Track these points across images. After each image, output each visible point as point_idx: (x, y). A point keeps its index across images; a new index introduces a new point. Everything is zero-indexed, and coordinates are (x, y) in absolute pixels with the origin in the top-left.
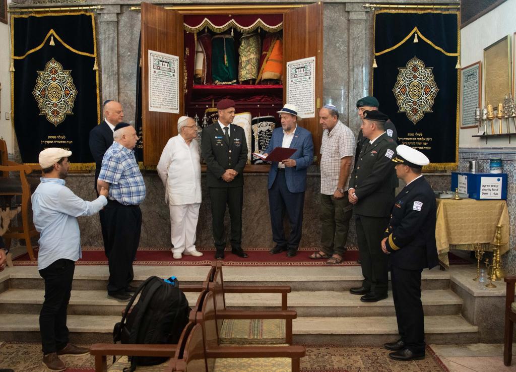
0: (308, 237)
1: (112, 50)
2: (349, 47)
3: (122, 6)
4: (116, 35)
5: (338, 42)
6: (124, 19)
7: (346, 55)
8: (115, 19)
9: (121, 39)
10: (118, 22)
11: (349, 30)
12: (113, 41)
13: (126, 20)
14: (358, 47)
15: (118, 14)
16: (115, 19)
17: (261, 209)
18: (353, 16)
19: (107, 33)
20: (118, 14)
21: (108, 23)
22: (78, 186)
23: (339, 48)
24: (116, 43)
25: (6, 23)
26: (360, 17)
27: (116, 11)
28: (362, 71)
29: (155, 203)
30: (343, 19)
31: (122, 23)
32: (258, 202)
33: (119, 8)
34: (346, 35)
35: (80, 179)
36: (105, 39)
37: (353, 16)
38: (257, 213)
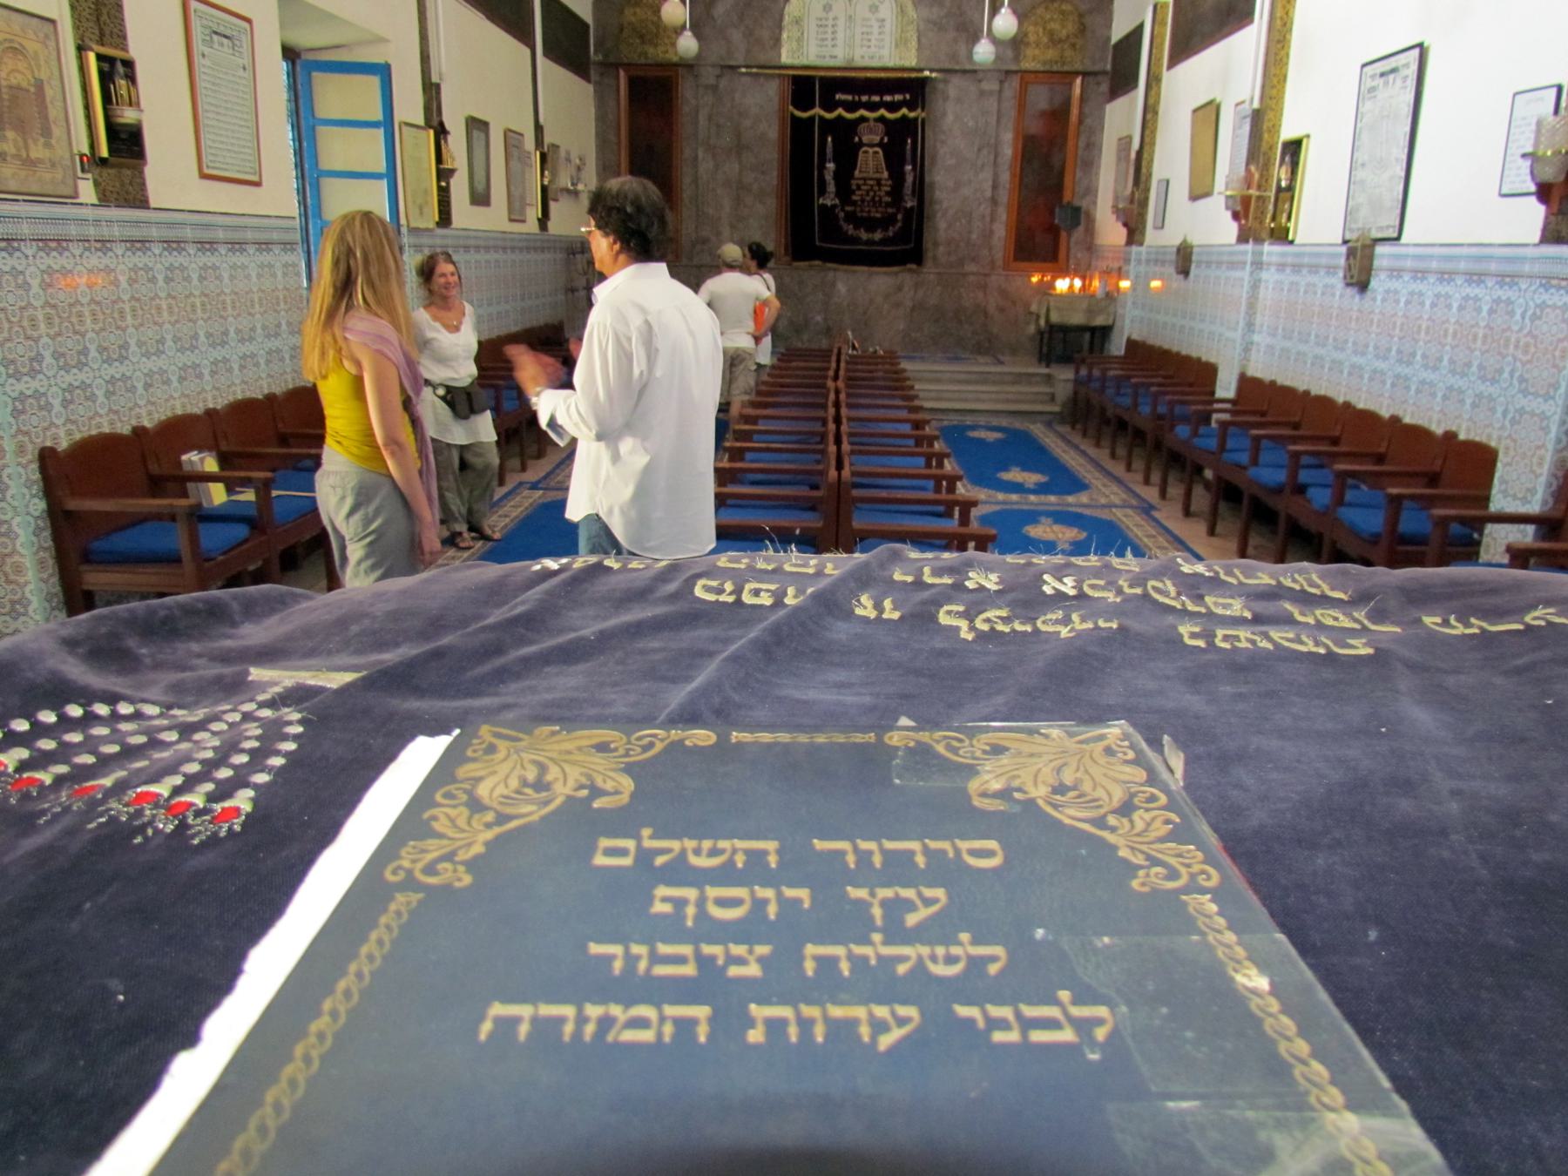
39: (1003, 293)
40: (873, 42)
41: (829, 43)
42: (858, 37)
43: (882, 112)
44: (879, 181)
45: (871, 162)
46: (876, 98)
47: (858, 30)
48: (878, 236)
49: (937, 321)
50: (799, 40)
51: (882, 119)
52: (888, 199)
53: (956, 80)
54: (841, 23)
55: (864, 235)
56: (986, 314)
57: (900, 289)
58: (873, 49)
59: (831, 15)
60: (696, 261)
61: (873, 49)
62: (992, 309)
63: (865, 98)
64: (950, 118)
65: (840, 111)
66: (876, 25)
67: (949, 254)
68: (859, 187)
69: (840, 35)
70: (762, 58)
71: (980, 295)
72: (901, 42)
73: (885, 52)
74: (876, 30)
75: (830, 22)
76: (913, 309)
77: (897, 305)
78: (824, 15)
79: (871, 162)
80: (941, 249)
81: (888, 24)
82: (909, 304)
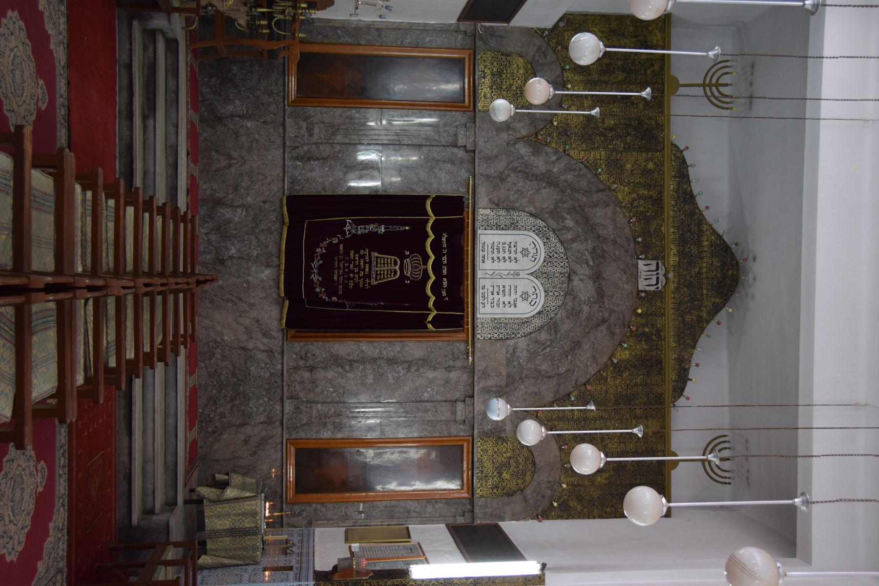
0: (211, 359)
1: (427, 139)
2: (427, 401)
3: (474, 151)
4: (443, 143)
5: (433, 390)
6: (461, 153)
7: (418, 399)
8: (459, 145)
9: (438, 149)
10: (456, 146)
11: (446, 401)
12: (436, 140)
13: (459, 156)
14: (427, 411)
15: (465, 147)
16: (459, 145)
17: (244, 305)
18: (460, 406)
19: (445, 135)
20: (465, 147)
21: (456, 135)
22: (272, 92)
23: (426, 391)
24: (434, 143)
25: (459, 20)
26: (459, 414)
27: (468, 145)
28: (400, 417)
29: (252, 182)
30: (457, 395)
31: (455, 150)
32: (252, 301)
33: (472, 149)
34: (439, 398)
35: (281, 94)
36: (439, 132)
37: (460, 406)
38: (240, 299)
39: (263, 442)
40: (496, 297)
41: (495, 255)
42: (500, 282)
43: (433, 278)
44: (369, 276)
45: (386, 268)
46: (445, 272)
47: (507, 283)
48: (315, 278)
49: (234, 374)
50: (498, 227)
51: (426, 277)
52: (351, 284)
53: (465, 377)
54: (513, 266)
55: (315, 264)
56: (242, 425)
57: (265, 334)
58: (491, 297)
59: (519, 256)
60: (289, 121)
61: (491, 297)
62: (248, 430)
63: (445, 259)
64: (430, 374)
65: (432, 237)
66: (512, 300)
67: (302, 382)
68: (361, 257)
69: (502, 265)
70: (482, 191)
71: (262, 418)
72: (497, 323)
73: (488, 308)
74: (507, 299)
75: (513, 255)
76: (244, 349)
77: (248, 331)
78: (519, 250)
79: (386, 268)
80: (307, 375)
81: (512, 310)
82: (251, 345)
